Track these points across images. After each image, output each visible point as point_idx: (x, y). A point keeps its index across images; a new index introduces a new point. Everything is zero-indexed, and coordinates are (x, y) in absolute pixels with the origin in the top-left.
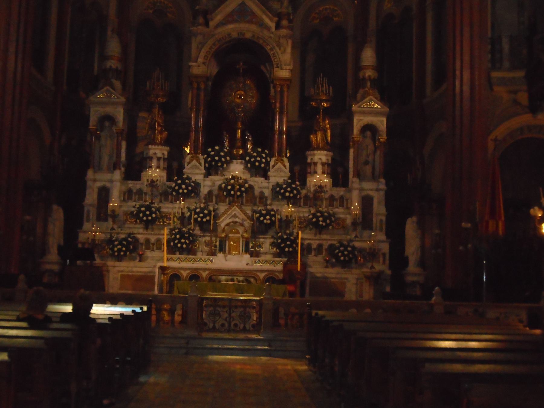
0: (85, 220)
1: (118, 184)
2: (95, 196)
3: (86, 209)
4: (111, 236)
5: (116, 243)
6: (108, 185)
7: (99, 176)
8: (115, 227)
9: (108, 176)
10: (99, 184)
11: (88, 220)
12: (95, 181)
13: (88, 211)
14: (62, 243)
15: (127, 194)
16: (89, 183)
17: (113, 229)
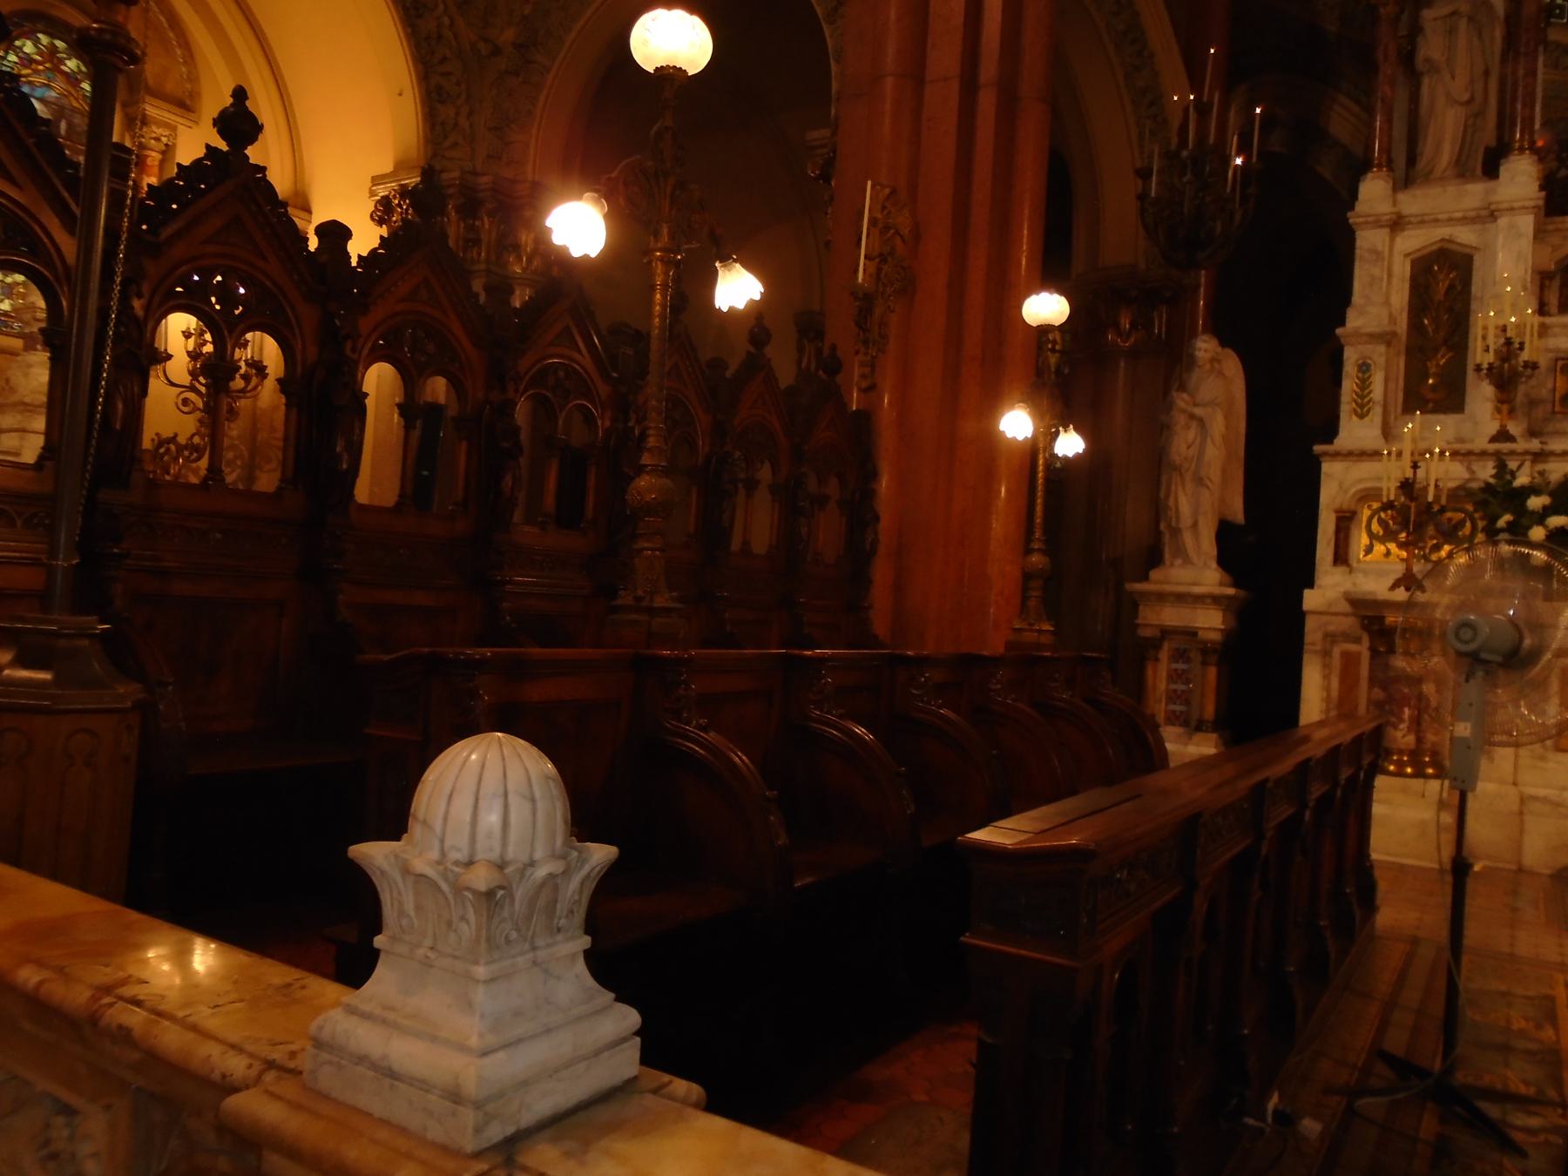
0: (1346, 407)
1: (1527, 223)
2: (1400, 297)
3: (1351, 356)
4: (1501, 467)
5: (1535, 503)
6: (1465, 236)
7: (1413, 203)
8: (1514, 428)
9: (1474, 193)
10: (1413, 241)
11: (1362, 412)
12: (1397, 224)
13: (1364, 368)
14: (1237, 512)
15: (1556, 284)
16: (1368, 239)
17: (1503, 436)
